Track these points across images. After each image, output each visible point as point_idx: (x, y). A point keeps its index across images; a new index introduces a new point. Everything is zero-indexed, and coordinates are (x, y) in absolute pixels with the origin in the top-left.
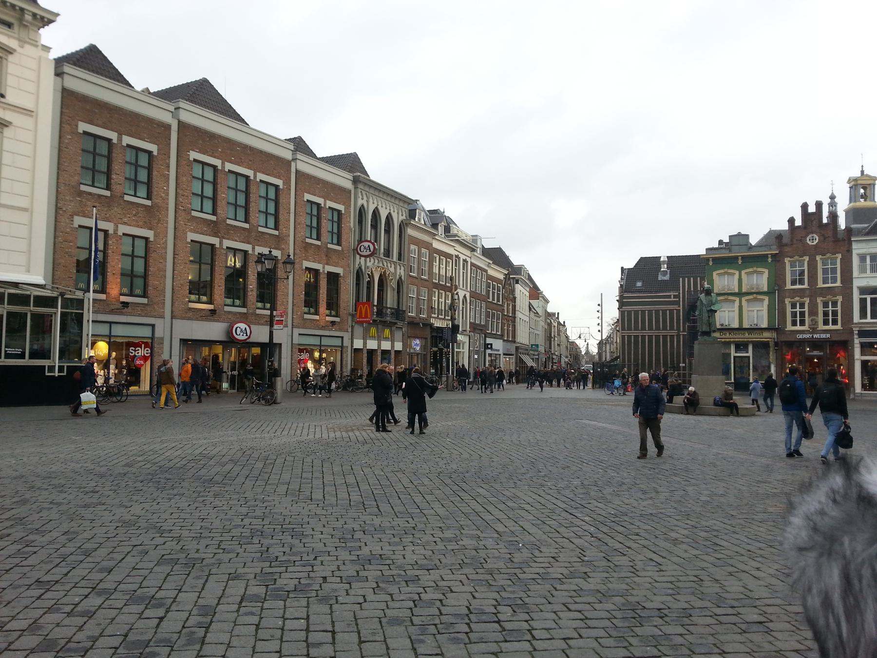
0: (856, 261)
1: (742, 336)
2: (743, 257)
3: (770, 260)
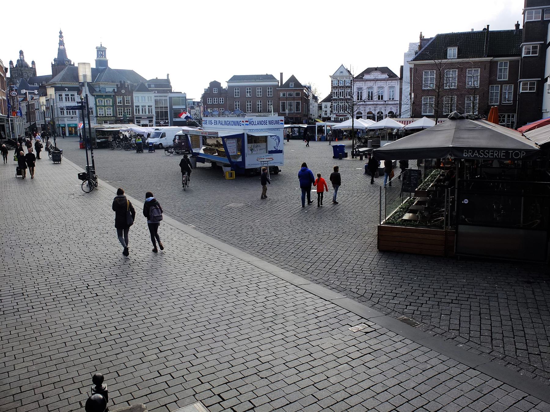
2: (105, 95)
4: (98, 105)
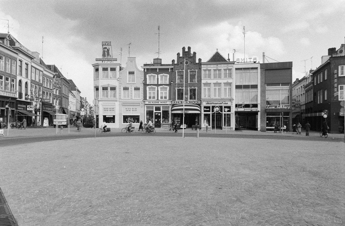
0: (203, 72)
2: (159, 69)
3: (170, 71)
4: (148, 83)
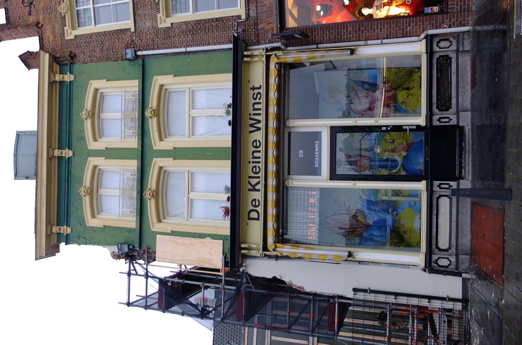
1: (262, 148)
3: (68, 78)
